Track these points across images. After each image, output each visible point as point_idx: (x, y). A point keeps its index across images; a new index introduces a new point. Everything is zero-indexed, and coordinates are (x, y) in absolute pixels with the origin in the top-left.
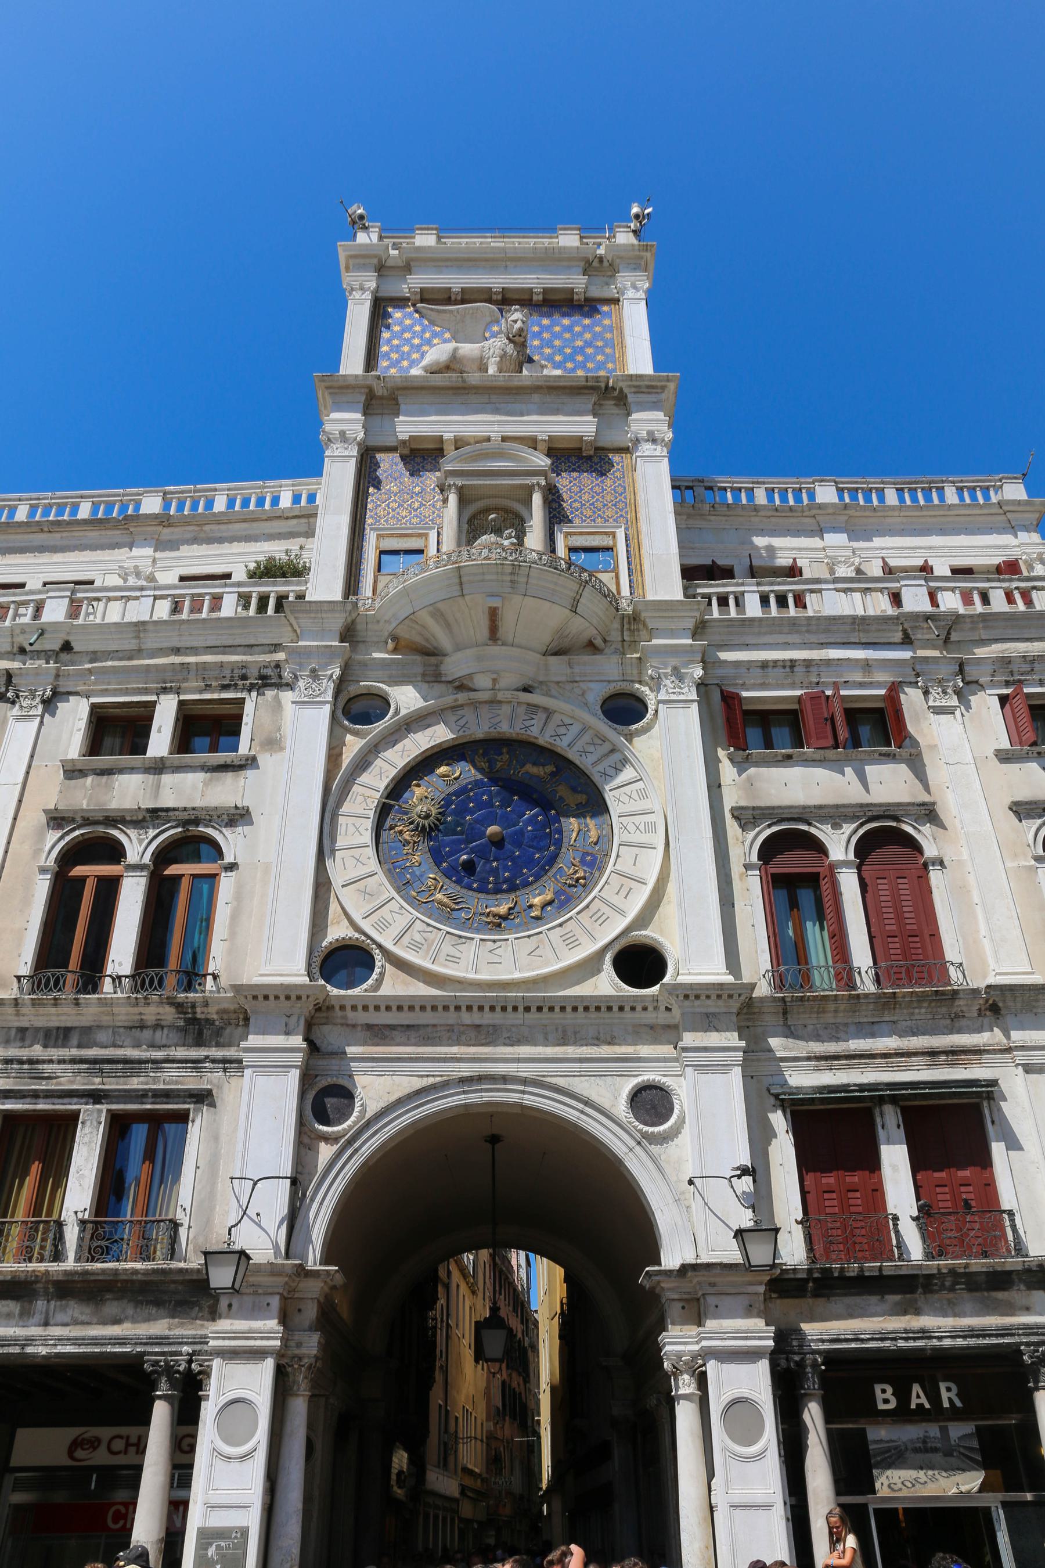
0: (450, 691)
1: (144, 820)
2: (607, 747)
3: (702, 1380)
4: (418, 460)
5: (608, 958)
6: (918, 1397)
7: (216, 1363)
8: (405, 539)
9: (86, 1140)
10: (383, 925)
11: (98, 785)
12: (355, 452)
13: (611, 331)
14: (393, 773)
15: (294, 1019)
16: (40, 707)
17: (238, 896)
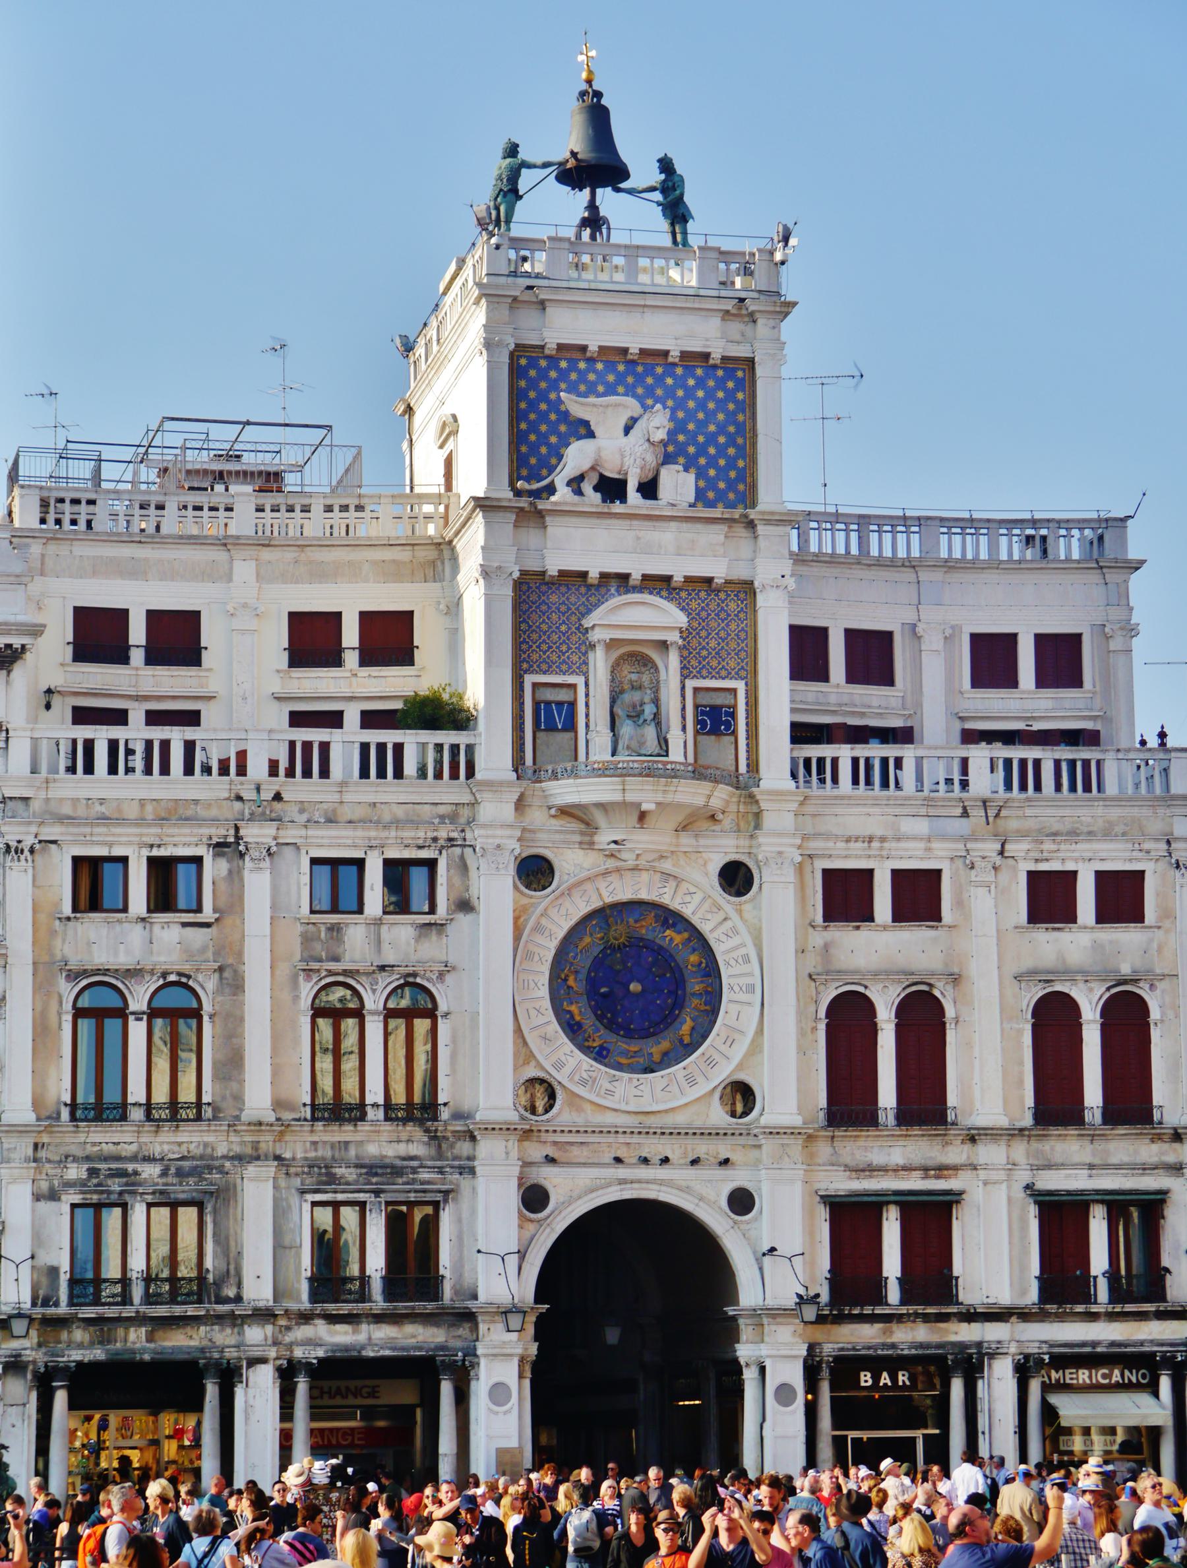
0: (602, 858)
1: (374, 972)
2: (721, 916)
3: (762, 1370)
4: (563, 589)
5: (717, 1095)
6: (885, 1379)
7: (483, 1362)
8: (557, 690)
9: (375, 1222)
10: (559, 1065)
11: (332, 938)
12: (510, 593)
13: (744, 411)
14: (561, 934)
15: (511, 1143)
16: (267, 859)
17: (454, 1039)
